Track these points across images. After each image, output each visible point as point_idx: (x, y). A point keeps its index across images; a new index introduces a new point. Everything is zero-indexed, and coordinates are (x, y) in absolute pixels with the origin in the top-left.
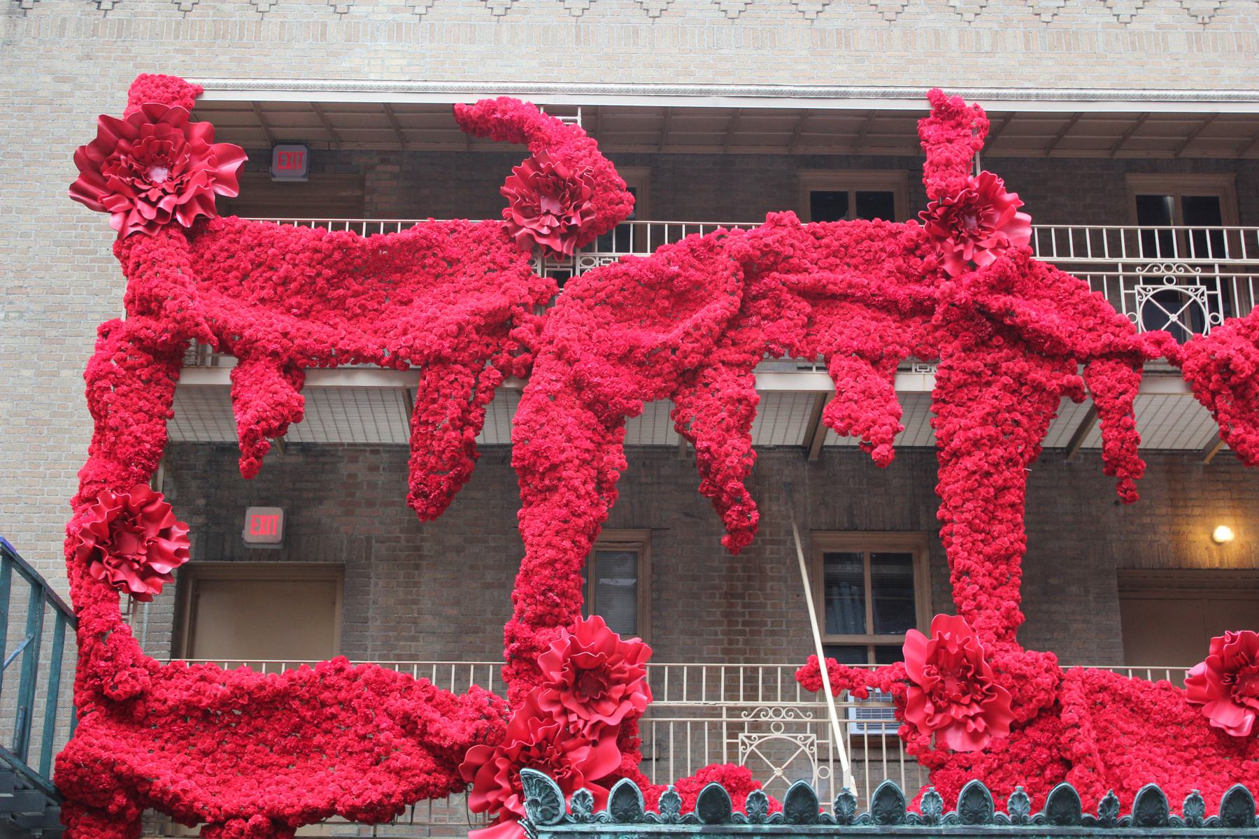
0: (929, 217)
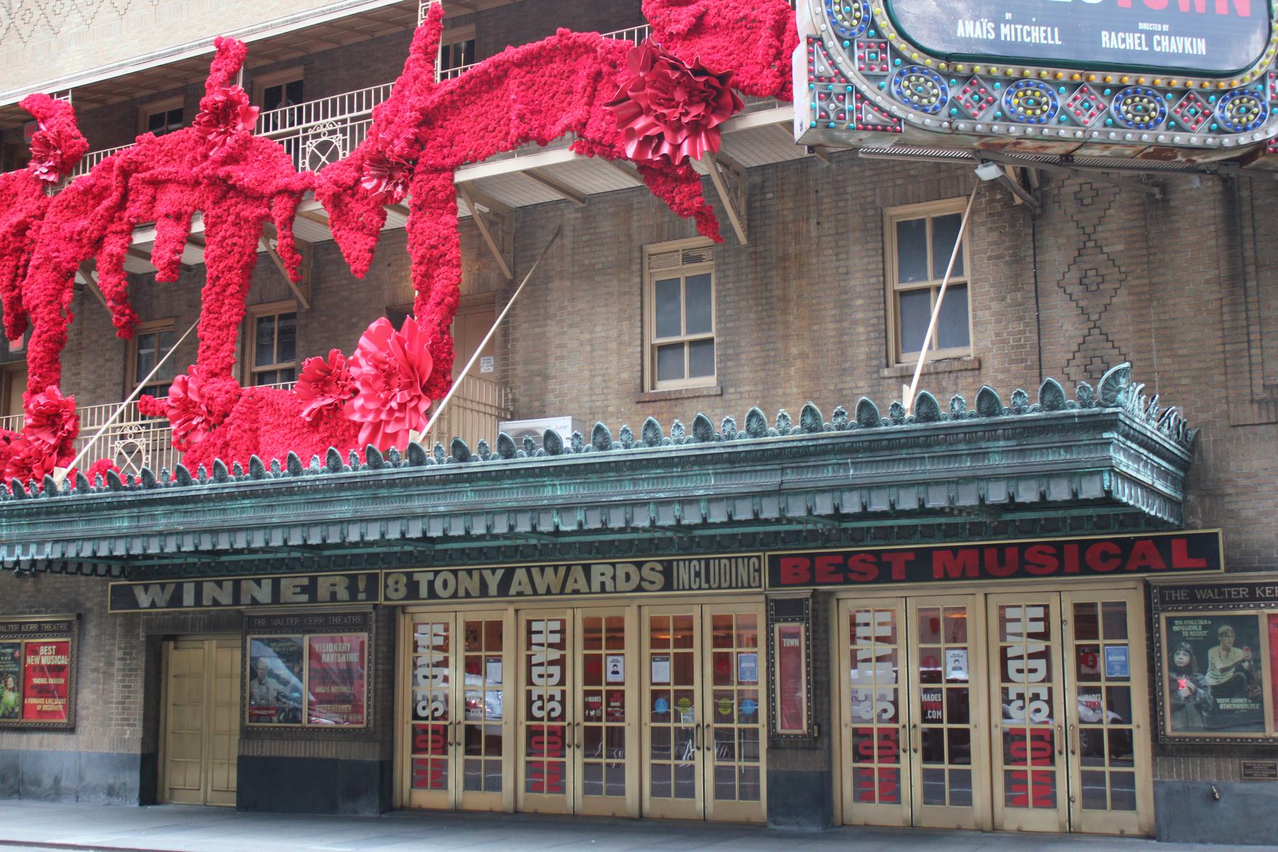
0: (199, 123)
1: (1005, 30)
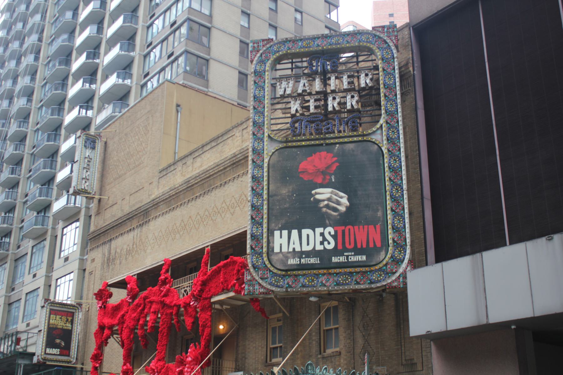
1: (302, 260)
